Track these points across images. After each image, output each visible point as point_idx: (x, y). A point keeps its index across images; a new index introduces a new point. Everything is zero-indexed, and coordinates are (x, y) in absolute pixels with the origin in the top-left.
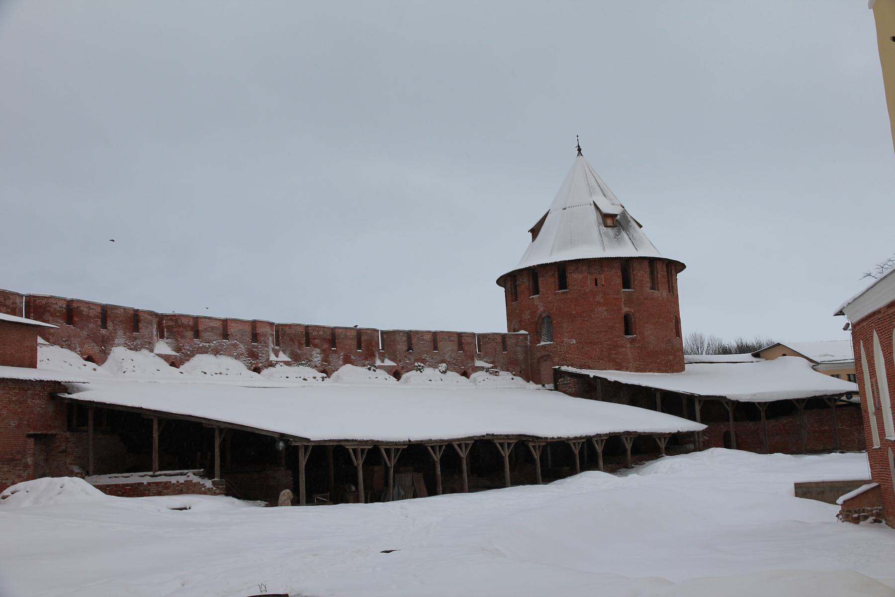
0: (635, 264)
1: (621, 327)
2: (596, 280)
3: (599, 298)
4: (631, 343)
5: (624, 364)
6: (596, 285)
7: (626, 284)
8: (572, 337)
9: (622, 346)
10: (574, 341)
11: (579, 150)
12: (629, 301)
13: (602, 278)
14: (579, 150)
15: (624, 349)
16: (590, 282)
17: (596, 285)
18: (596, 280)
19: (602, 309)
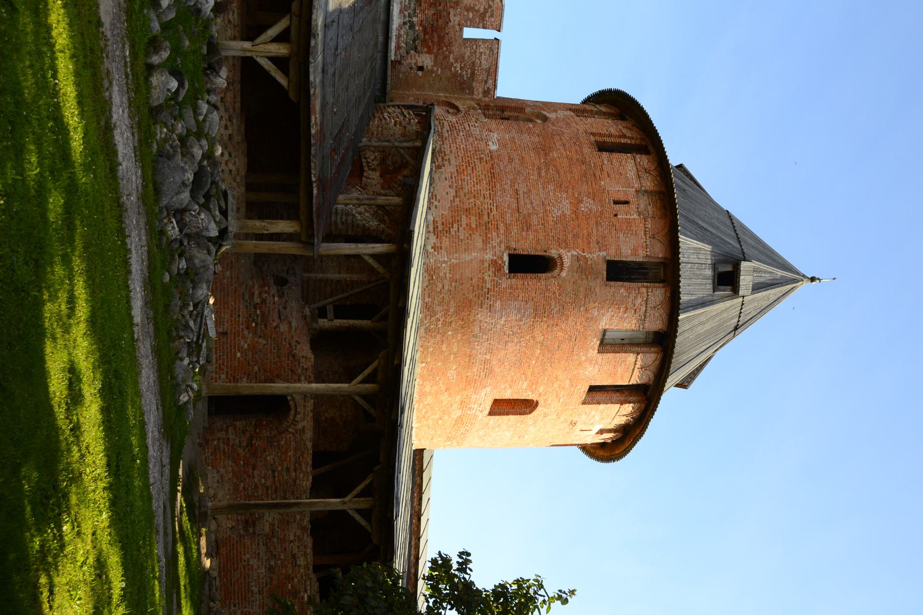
0: (658, 294)
1: (527, 246)
2: (627, 203)
3: (588, 205)
4: (494, 263)
5: (446, 242)
6: (616, 203)
7: (618, 271)
8: (502, 145)
9: (486, 241)
10: (494, 147)
11: (813, 279)
12: (583, 268)
13: (629, 214)
14: (813, 279)
15: (479, 244)
16: (617, 190)
17: (616, 202)
18: (627, 203)
19: (566, 207)
